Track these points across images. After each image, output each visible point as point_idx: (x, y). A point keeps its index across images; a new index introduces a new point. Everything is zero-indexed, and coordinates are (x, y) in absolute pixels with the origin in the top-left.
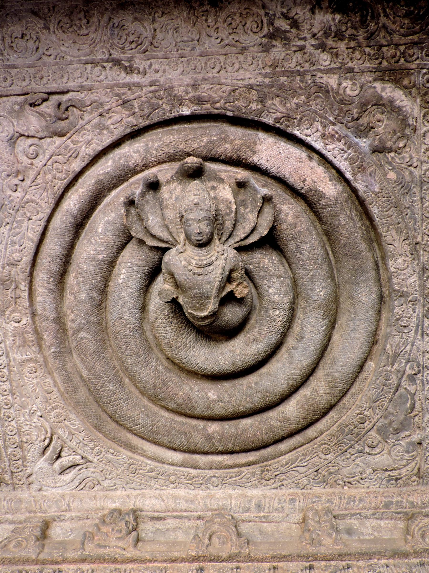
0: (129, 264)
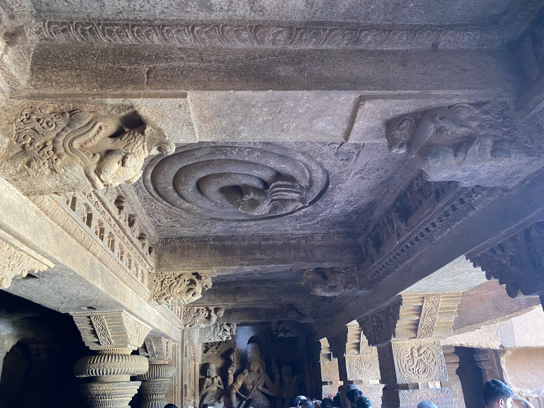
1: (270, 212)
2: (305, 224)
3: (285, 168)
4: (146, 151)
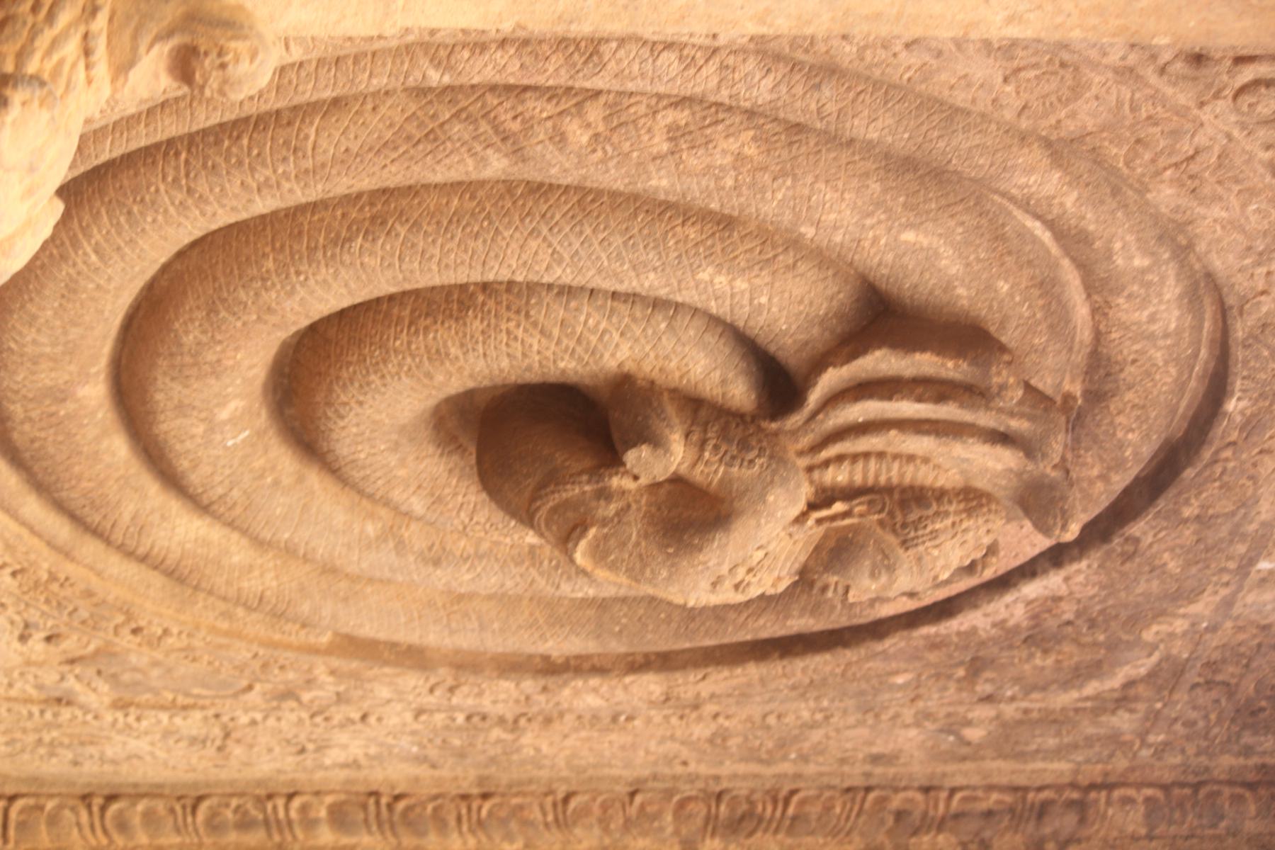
0: (764, 300)
1: (805, 579)
2: (1036, 702)
3: (929, 255)
4: (102, 70)
